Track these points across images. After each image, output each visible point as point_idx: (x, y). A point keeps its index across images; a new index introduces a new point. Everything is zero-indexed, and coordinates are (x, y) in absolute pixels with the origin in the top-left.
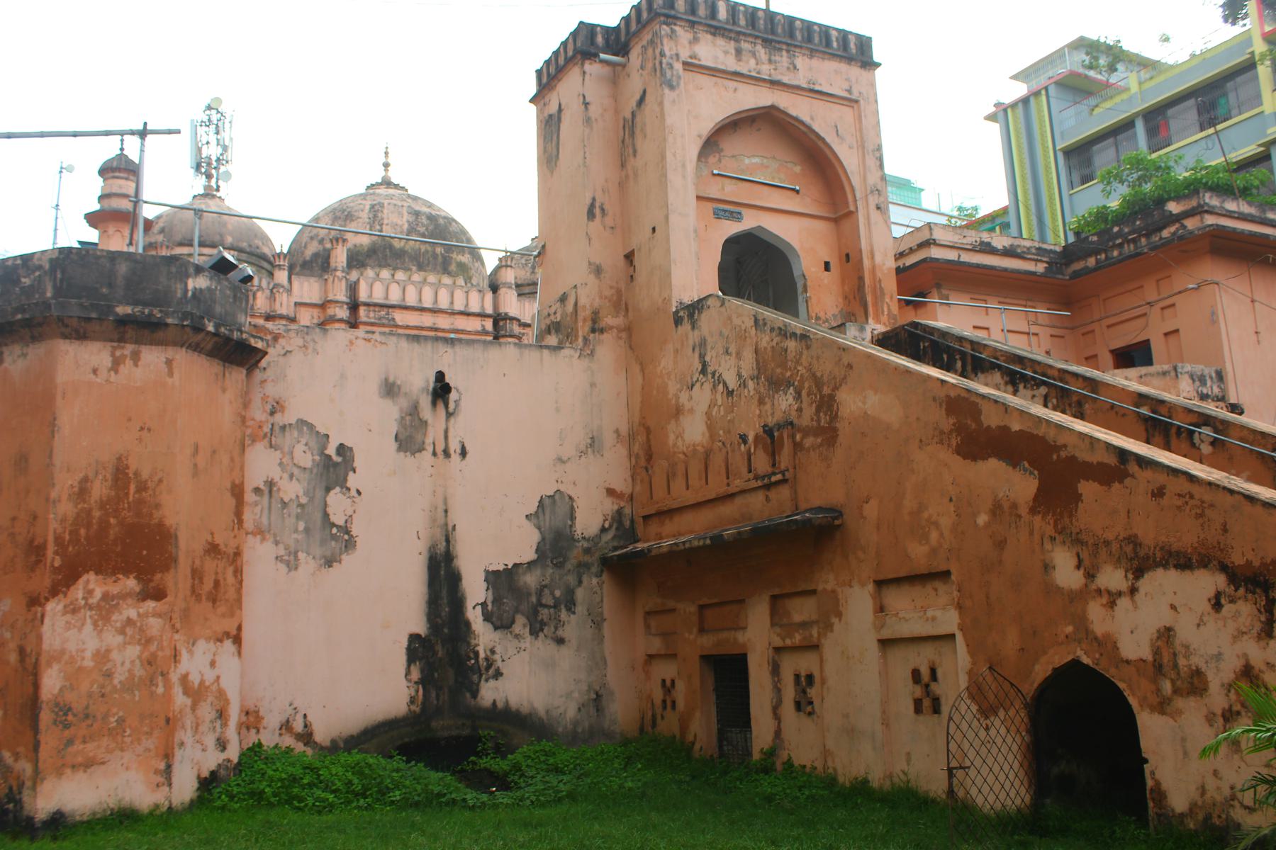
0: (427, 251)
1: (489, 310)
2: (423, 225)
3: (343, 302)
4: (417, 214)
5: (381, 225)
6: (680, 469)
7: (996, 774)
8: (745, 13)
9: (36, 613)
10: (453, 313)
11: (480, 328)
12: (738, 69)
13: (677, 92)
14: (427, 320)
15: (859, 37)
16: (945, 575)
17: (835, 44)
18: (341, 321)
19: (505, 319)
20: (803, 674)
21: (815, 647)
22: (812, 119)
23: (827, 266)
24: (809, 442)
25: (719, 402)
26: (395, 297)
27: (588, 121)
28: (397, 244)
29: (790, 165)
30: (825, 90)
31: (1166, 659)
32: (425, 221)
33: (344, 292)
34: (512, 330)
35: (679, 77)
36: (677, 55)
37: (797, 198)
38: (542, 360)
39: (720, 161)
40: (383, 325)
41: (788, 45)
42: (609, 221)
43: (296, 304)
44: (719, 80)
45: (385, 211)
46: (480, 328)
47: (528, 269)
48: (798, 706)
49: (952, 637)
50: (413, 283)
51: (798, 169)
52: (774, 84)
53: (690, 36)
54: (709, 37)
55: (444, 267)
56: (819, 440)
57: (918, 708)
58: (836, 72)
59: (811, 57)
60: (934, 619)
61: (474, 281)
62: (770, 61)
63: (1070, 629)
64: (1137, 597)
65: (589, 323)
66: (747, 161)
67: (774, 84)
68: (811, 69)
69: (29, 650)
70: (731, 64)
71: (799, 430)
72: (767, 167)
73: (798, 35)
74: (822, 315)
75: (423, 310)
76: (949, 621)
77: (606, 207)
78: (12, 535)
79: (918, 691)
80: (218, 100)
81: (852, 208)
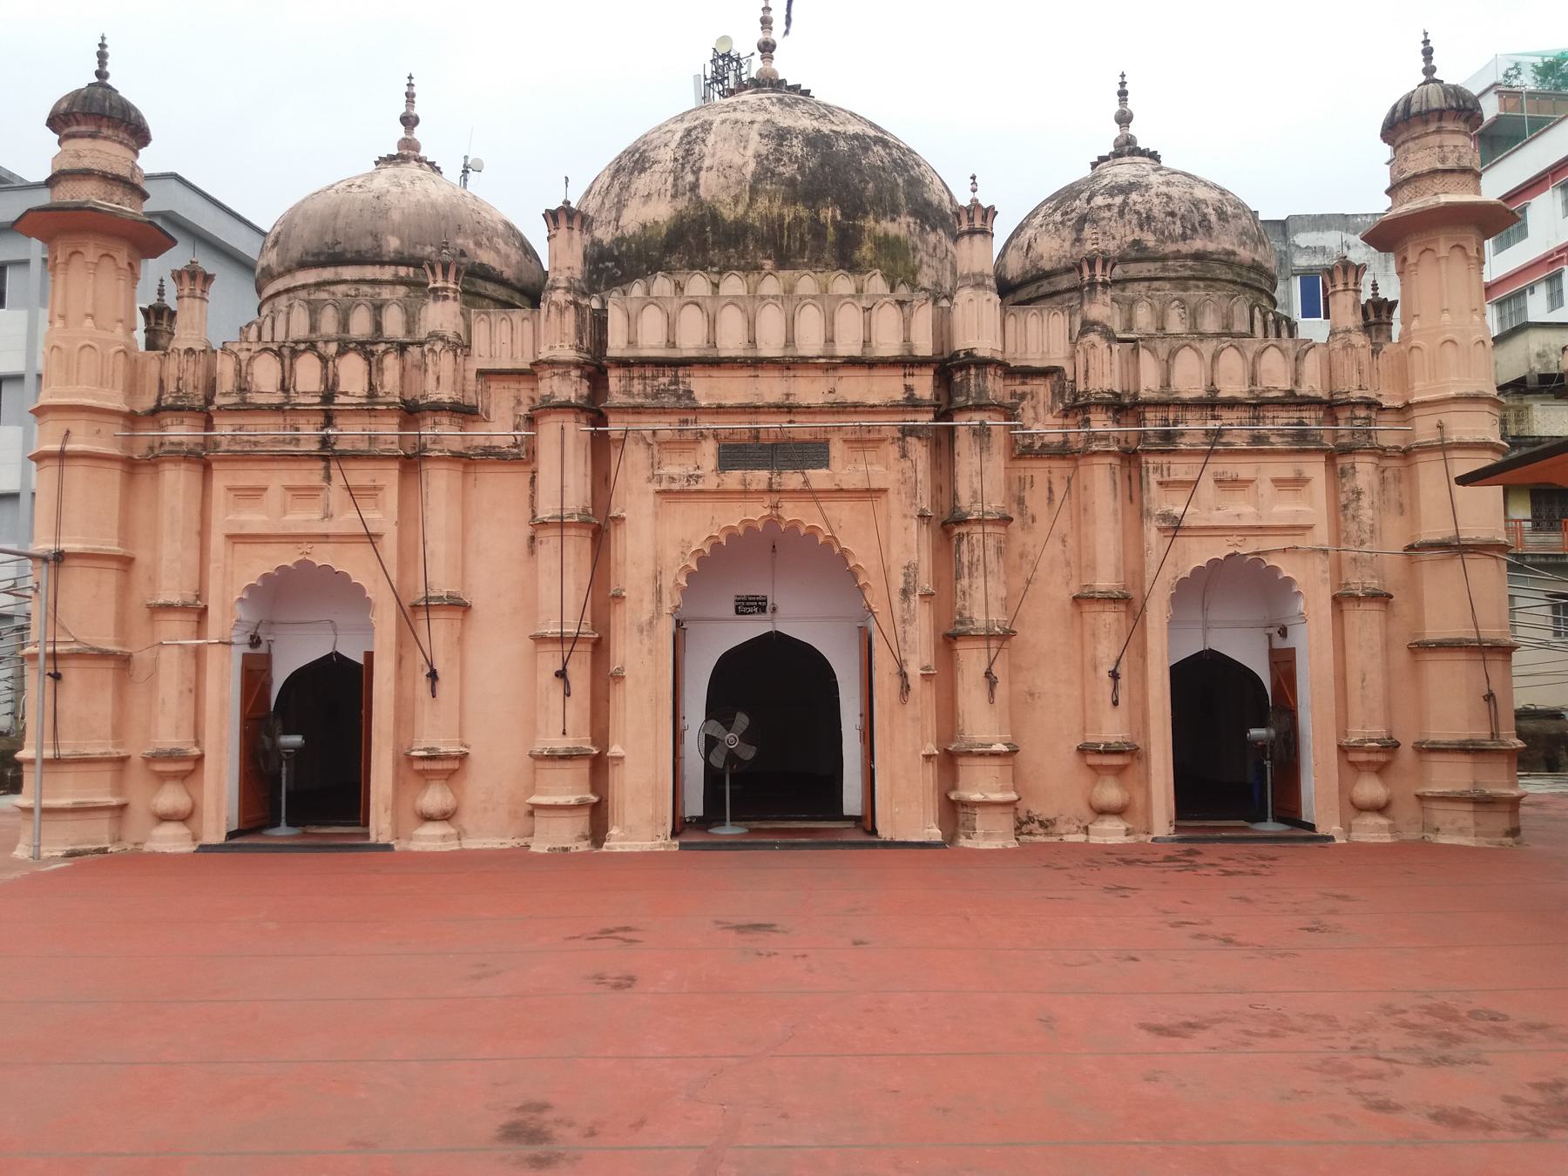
0: (798, 220)
1: (924, 346)
2: (793, 159)
3: (567, 364)
4: (782, 135)
5: (696, 173)
10: (834, 364)
11: (900, 396)
14: (771, 388)
18: (565, 407)
19: (965, 366)
26: (691, 341)
28: (729, 214)
32: (797, 147)
33: (571, 338)
34: (982, 392)
40: (662, 410)
43: (482, 373)
45: (711, 139)
46: (900, 396)
47: (1067, 233)
50: (733, 301)
55: (843, 252)
61: (925, 280)
75: (756, 364)
80: (725, 39)
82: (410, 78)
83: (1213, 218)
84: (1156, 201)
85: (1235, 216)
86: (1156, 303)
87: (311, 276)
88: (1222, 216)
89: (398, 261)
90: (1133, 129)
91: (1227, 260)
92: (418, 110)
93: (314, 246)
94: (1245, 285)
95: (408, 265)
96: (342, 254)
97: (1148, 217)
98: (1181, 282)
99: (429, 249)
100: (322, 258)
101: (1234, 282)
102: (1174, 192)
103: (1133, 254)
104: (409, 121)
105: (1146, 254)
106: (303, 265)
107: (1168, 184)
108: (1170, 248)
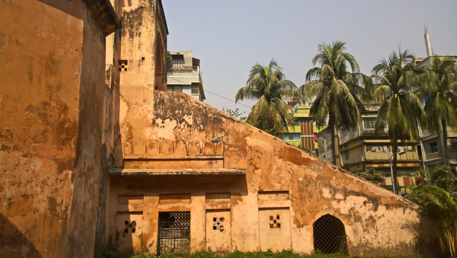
6: (156, 146)
7: (304, 242)
9: (67, 175)
16: (287, 192)
20: (219, 217)
21: (229, 210)
24: (231, 149)
25: (182, 127)
31: (353, 214)
48: (215, 228)
49: (288, 208)
56: (237, 149)
57: (271, 226)
60: (282, 203)
63: (327, 207)
64: (346, 201)
69: (59, 201)
71: (227, 145)
76: (288, 203)
78: (44, 116)
79: (272, 222)
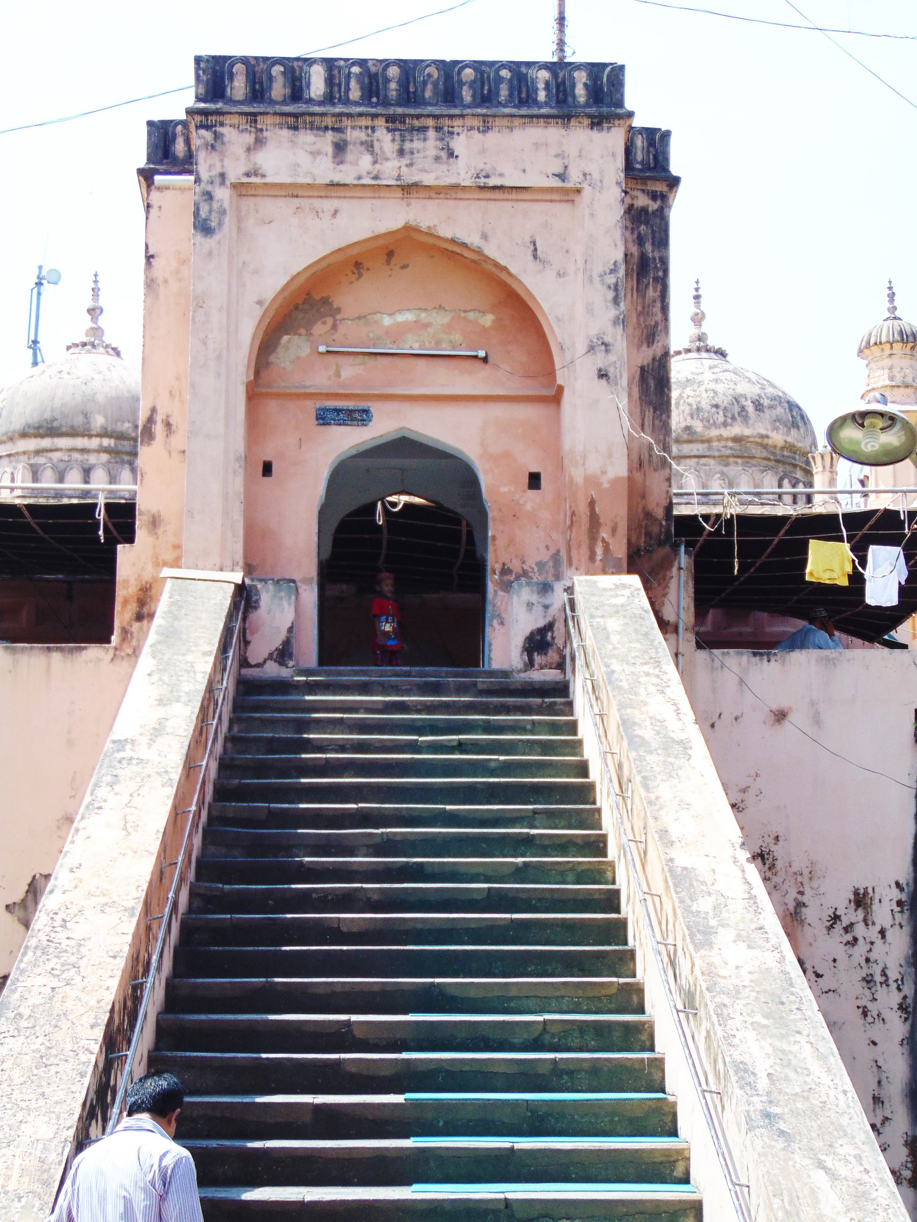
8: (359, 77)
12: (337, 178)
13: (217, 237)
15: (595, 69)
17: (542, 96)
22: (485, 237)
23: (534, 480)
27: (150, 284)
29: (471, 316)
30: (508, 183)
35: (223, 212)
36: (223, 176)
37: (484, 372)
38: (48, 669)
39: (334, 327)
41: (436, 117)
42: (178, 442)
44: (305, 202)
51: (488, 320)
52: (409, 189)
53: (249, 139)
54: (286, 133)
58: (537, 145)
59: (486, 129)
62: (401, 152)
65: (133, 607)
66: (387, 321)
67: (409, 189)
68: (483, 151)
70: (325, 170)
72: (427, 325)
73: (467, 95)
74: (516, 566)
77: (172, 421)
81: (560, 381)
82: (96, 275)
83: (750, 408)
84: (705, 395)
85: (771, 407)
86: (703, 475)
87: (32, 444)
88: (758, 406)
89: (104, 434)
90: (706, 327)
91: (762, 442)
92: (101, 303)
93: (35, 419)
94: (777, 461)
95: (110, 437)
96: (59, 428)
97: (698, 409)
98: (724, 460)
99: (127, 425)
100: (41, 431)
101: (769, 459)
102: (720, 388)
103: (685, 437)
104: (94, 312)
105: (695, 437)
106: (24, 435)
107: (716, 381)
108: (714, 433)
